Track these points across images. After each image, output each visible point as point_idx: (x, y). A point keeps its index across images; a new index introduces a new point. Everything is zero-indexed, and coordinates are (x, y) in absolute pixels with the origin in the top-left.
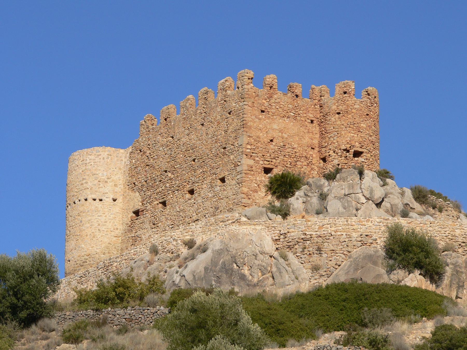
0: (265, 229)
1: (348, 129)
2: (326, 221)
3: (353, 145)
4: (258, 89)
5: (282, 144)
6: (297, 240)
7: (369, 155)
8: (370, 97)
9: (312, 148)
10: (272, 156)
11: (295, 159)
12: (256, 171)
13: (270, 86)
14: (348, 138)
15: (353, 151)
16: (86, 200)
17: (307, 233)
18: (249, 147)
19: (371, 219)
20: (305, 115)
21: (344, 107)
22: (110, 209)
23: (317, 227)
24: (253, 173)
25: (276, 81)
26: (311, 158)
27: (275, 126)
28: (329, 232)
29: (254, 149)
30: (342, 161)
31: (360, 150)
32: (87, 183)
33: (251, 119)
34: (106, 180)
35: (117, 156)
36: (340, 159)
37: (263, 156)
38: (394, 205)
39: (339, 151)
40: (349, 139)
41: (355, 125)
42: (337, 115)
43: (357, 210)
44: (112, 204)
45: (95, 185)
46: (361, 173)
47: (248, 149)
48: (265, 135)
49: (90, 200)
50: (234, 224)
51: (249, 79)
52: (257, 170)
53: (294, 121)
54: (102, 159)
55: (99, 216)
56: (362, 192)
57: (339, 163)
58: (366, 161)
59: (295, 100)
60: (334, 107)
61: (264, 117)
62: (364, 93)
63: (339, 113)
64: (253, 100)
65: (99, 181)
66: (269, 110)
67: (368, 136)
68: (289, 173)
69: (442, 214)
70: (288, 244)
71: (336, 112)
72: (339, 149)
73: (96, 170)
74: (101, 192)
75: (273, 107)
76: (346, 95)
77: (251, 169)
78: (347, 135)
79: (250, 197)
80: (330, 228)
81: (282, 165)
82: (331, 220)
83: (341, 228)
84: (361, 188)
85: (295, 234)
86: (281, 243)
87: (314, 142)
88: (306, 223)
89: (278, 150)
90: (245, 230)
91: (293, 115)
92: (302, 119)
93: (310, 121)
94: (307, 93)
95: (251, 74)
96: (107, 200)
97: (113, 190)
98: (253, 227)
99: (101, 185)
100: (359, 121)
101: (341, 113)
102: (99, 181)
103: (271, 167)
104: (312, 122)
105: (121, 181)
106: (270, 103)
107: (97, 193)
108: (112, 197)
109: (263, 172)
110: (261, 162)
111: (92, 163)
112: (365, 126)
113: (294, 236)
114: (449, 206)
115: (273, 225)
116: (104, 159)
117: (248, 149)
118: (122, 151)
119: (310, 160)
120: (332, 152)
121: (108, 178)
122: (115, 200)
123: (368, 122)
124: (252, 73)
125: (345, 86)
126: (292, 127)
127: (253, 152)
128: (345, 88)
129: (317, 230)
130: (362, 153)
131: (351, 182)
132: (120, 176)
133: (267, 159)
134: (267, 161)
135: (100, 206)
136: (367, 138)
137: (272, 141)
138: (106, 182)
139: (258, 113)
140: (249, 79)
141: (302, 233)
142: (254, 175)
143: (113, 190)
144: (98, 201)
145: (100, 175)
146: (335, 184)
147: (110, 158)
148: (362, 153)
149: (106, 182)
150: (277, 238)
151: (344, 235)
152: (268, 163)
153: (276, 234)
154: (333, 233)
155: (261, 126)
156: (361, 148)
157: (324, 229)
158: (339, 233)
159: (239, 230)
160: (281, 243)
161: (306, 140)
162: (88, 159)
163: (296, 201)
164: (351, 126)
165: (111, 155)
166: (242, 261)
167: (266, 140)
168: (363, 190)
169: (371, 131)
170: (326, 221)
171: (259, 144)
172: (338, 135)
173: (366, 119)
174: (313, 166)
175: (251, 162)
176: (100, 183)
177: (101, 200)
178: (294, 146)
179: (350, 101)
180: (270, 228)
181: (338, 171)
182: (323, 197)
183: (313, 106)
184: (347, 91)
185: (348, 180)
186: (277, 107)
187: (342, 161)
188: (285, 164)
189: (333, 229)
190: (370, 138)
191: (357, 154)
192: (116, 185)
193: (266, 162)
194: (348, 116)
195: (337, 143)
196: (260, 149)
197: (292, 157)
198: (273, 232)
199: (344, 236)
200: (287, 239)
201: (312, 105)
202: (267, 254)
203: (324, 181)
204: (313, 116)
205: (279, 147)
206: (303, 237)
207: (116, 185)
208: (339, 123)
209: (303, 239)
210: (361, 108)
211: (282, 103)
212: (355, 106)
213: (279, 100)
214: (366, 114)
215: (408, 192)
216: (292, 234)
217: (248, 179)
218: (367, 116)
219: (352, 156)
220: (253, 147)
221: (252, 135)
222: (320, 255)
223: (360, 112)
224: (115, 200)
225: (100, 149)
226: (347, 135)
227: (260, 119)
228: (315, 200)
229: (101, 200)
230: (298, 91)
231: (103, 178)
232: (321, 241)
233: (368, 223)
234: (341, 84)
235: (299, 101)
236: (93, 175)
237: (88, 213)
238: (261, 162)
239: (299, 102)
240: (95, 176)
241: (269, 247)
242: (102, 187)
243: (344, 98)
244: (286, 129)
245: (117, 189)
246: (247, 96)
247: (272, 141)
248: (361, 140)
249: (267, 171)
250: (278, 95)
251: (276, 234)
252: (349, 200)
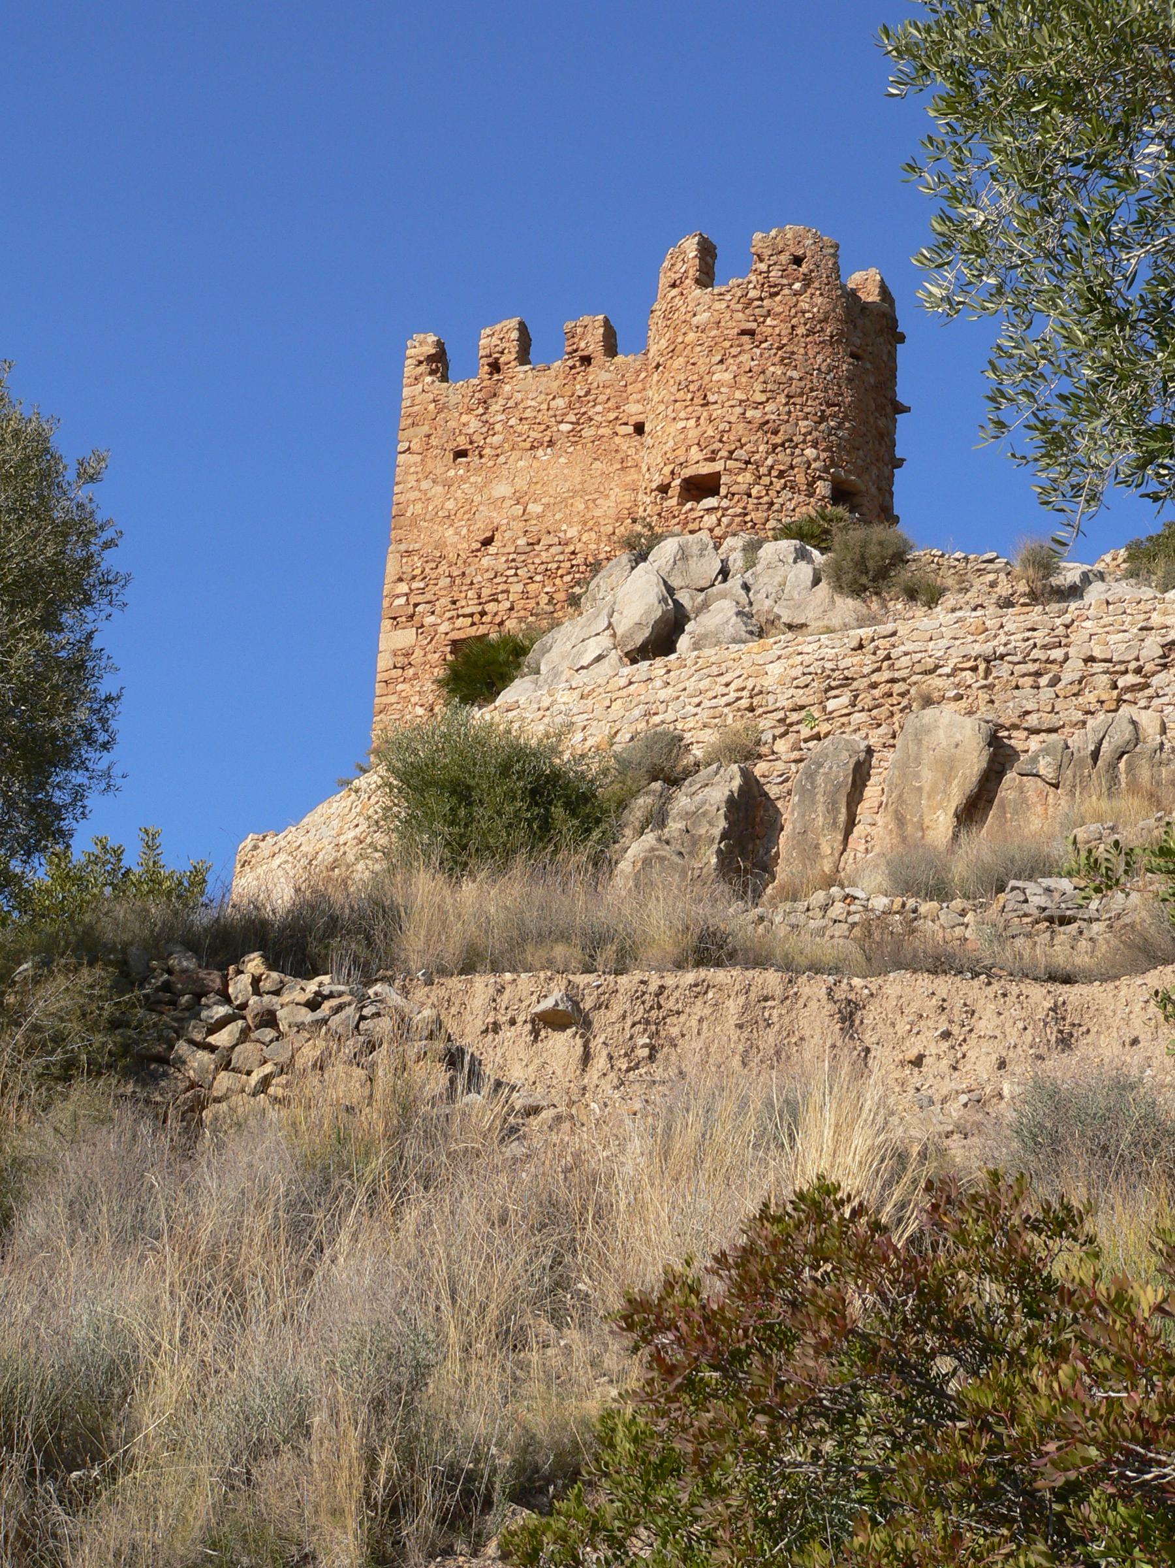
5: (522, 542)
10: (485, 592)
13: (491, 360)
20: (612, 416)
29: (422, 592)
31: (706, 469)
51: (420, 362)
64: (426, 429)
75: (498, 427)
91: (570, 427)
92: (601, 431)
93: (630, 429)
95: (422, 345)
110: (443, 628)
123: (744, 357)
126: (559, 470)
133: (460, 612)
134: (464, 616)
136: (733, 419)
140: (420, 362)
148: (717, 476)
155: (450, 505)
167: (465, 545)
171: (444, 567)
178: (569, 535)
186: (512, 422)
193: (460, 622)
197: (560, 572)
211: (530, 403)
212: (695, 321)
214: (736, 331)
220: (415, 585)
221: (417, 546)
227: (448, 484)
248: (710, 432)
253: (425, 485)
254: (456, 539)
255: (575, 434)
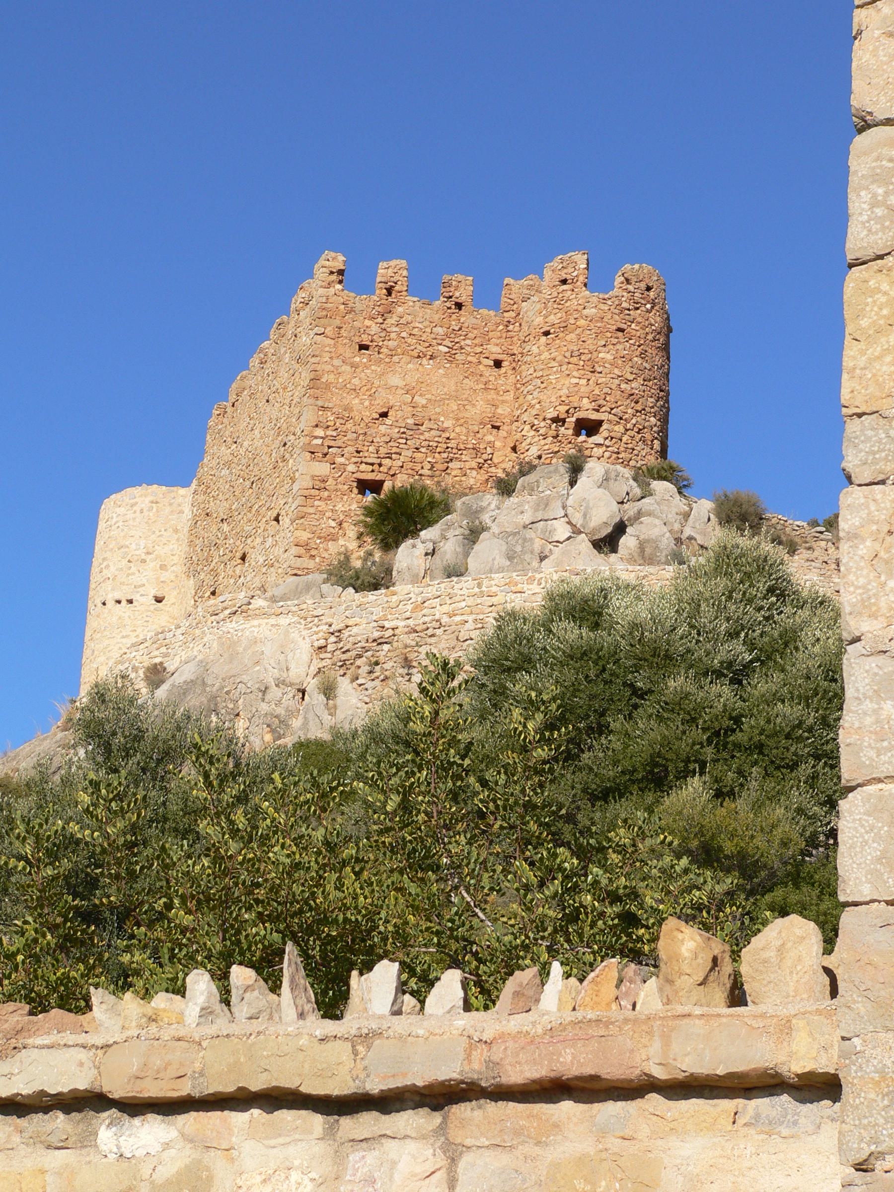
0: (300, 623)
1: (564, 368)
2: (431, 591)
3: (576, 405)
4: (353, 294)
5: (410, 421)
6: (363, 644)
7: (620, 428)
8: (631, 288)
9: (494, 427)
10: (383, 451)
11: (445, 455)
12: (336, 490)
13: (387, 286)
14: (565, 388)
15: (574, 419)
16: (104, 604)
17: (387, 624)
18: (320, 432)
19: (538, 576)
20: (479, 350)
21: (559, 315)
22: (147, 619)
23: (410, 607)
24: (326, 494)
25: (405, 273)
26: (489, 450)
27: (395, 380)
28: (437, 617)
29: (334, 439)
30: (546, 447)
31: (594, 416)
32: (107, 567)
33: (328, 368)
34: (143, 557)
35: (171, 504)
36: (543, 442)
37: (358, 452)
38: (647, 541)
39: (543, 424)
40: (565, 391)
41: (583, 357)
42: (543, 339)
43: (542, 559)
44: (152, 608)
45: (121, 569)
46: (575, 469)
47: (316, 437)
48: (367, 403)
49: (110, 603)
50: (235, 618)
51: (332, 273)
52: (340, 486)
53: (448, 365)
54: (138, 512)
55: (123, 637)
56: (566, 515)
57: (539, 453)
58: (607, 442)
59: (454, 316)
60: (539, 320)
61: (365, 360)
62: (619, 279)
63: (547, 333)
64: (338, 322)
65: (129, 561)
66: (380, 344)
67: (617, 382)
68: (424, 488)
69: (796, 557)
70: (344, 657)
71: (542, 331)
72: (541, 418)
73: (125, 537)
74: (131, 584)
75: (393, 335)
76: (565, 287)
77: (323, 485)
78: (562, 382)
79: (313, 552)
80: (438, 606)
81: (410, 472)
82: (442, 585)
83: (463, 604)
84: (564, 507)
85: (362, 630)
86: (329, 655)
87: (499, 411)
88: (385, 599)
89: (398, 435)
90: (256, 630)
91: (447, 350)
92: (469, 358)
93: (492, 363)
94: (488, 295)
95: (338, 261)
96: (142, 599)
97: (157, 579)
98: (273, 621)
99: (133, 569)
100: (591, 347)
101: (552, 331)
102: (129, 561)
103: (379, 477)
104: (498, 364)
105: (176, 558)
106: (383, 326)
107: (124, 587)
108: (153, 592)
109: (355, 491)
110: (351, 468)
111: (120, 524)
112: (609, 357)
113: (356, 635)
114: (822, 536)
115: (316, 613)
116: (142, 511)
117: (316, 437)
118: (182, 491)
119: (485, 456)
120: (527, 427)
121: (148, 553)
122: (159, 600)
123: (619, 347)
124: (341, 258)
125: (565, 264)
126: (440, 378)
127: (332, 443)
128: (565, 271)
129: (408, 614)
130: (600, 423)
131: (548, 492)
132: (176, 546)
133: (364, 460)
134: (366, 463)
135: (128, 614)
136: (613, 387)
137: (384, 415)
138: (144, 561)
139: (350, 352)
140: (332, 273)
141: (375, 624)
142: (329, 498)
143: (157, 579)
144: (124, 603)
145: (133, 546)
146: (514, 500)
147: (155, 510)
148: (600, 423)
149: (144, 561)
150: (322, 642)
151: (470, 621)
152: (371, 468)
153: (321, 634)
154: (445, 620)
155: (356, 381)
156: (598, 411)
157: (425, 611)
158: (458, 618)
159: (243, 630)
160: (329, 655)
161: (479, 408)
162: (115, 515)
163: (409, 555)
164: (571, 360)
165: (157, 502)
166: (231, 706)
167: (368, 413)
168: (570, 511)
169: (629, 370)
170: (431, 591)
171: (349, 425)
172: (543, 386)
173: (615, 341)
174: (493, 470)
175: (323, 468)
176: (131, 565)
177: (130, 602)
178: (445, 425)
179: (574, 301)
180: (309, 620)
181: (526, 469)
182: (474, 534)
183: (501, 327)
184: (568, 277)
185: (540, 489)
186: (404, 334)
187: (546, 447)
188: (417, 469)
189: (445, 609)
190: (623, 386)
191: (589, 427)
192: (163, 567)
193: (363, 467)
194: (568, 338)
195: (538, 406)
196: (350, 436)
197: (438, 450)
198: (315, 629)
199: (470, 625)
200: (341, 645)
201: (498, 325)
202: (291, 685)
203: (491, 499)
204: (500, 351)
205: (402, 430)
206: (376, 634)
207: (163, 567)
208: (546, 355)
209: (375, 640)
210: (601, 313)
211: (417, 325)
212: (585, 312)
213: (410, 318)
214: (615, 327)
215: (704, 507)
216: (355, 630)
217: (312, 510)
218: (620, 334)
219: (571, 432)
220: (329, 433)
221: (330, 405)
222: (407, 678)
223: (599, 325)
224: (159, 600)
225: (136, 491)
226: (562, 382)
227: (355, 366)
228: (450, 548)
229: (130, 602)
230: (464, 293)
231: (137, 552)
232: (414, 643)
233: (531, 586)
234: (556, 263)
235: (466, 317)
236: (119, 549)
237: (105, 633)
238: (351, 468)
239: (462, 320)
240: (122, 550)
241: (302, 665)
242: (133, 574)
243: (561, 295)
244: (423, 385)
245: (167, 576)
246: (324, 313)
247: (384, 415)
248: (597, 392)
249: (364, 486)
250: (409, 307)
251: (321, 634)
252: (528, 536)
253: (337, 362)
254: (363, 408)
255: (451, 357)
